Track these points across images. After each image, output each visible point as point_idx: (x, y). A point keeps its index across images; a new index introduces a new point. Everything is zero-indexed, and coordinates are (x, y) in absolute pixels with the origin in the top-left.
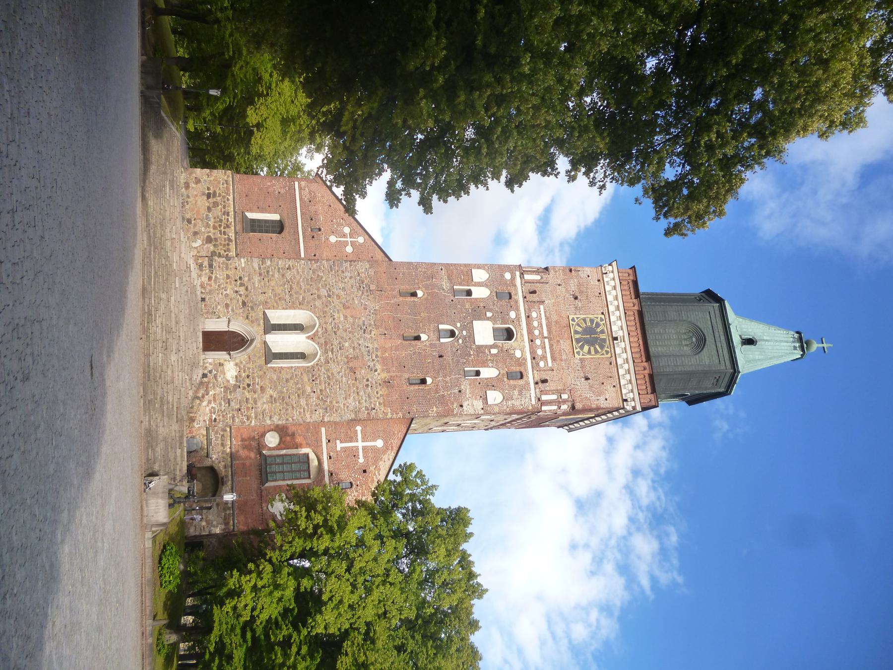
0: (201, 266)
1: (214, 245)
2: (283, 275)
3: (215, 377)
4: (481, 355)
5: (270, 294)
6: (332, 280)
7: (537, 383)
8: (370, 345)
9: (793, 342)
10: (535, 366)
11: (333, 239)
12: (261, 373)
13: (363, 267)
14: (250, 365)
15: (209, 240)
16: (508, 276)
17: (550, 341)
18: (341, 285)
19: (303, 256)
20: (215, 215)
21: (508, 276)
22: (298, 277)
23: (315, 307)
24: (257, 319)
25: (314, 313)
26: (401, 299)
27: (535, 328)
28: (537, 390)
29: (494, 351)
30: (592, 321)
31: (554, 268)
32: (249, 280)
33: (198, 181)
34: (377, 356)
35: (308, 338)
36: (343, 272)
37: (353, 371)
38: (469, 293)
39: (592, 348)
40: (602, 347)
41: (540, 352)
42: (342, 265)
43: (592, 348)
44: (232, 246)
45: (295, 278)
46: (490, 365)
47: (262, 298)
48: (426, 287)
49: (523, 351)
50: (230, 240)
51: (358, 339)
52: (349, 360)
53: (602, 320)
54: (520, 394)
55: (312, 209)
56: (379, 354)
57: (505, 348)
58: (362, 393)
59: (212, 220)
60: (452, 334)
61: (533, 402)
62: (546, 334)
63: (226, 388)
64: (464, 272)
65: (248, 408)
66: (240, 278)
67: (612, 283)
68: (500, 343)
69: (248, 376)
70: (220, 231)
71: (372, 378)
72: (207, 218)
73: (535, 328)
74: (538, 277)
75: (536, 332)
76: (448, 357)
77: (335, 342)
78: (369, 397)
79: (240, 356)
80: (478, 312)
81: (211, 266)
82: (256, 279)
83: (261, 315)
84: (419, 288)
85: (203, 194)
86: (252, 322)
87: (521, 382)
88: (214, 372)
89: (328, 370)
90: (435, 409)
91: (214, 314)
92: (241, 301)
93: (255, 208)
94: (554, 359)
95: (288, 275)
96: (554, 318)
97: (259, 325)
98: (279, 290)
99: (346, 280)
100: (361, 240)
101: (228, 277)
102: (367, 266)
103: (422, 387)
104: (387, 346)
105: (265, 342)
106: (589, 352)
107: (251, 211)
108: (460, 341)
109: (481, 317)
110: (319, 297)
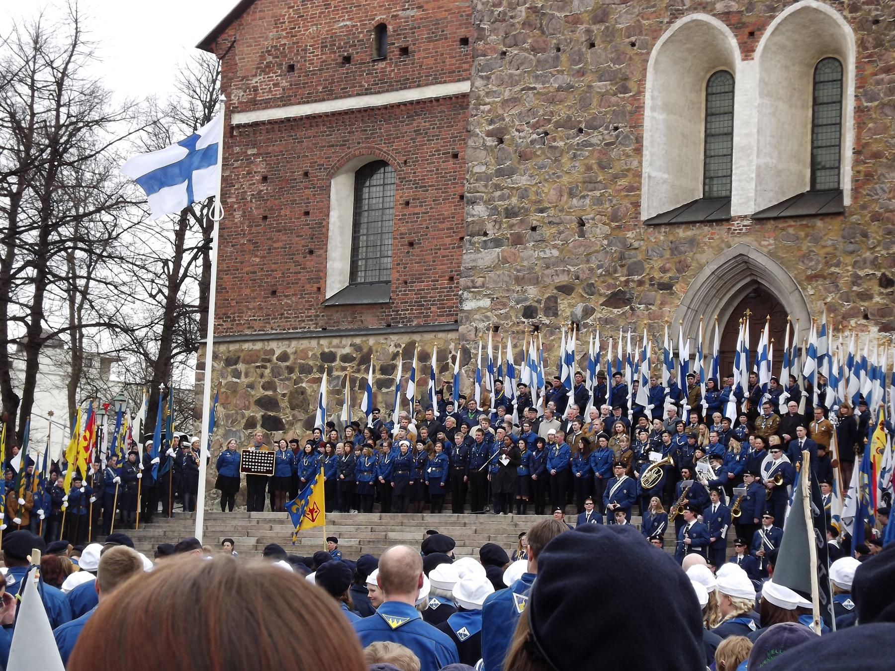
2: (523, 157)
14: (845, 274)
19: (463, 87)
22: (530, 100)
23: (637, 29)
24: (675, 250)
25: (656, 33)
32: (536, 281)
35: (747, 51)
47: (598, 231)
55: (315, 58)
66: (529, 312)
82: (530, 254)
83: (660, 236)
86: (682, 267)
93: (311, 263)
95: (522, 135)
97: (692, 242)
98: (573, 171)
105: (759, 219)
107: (319, 277)
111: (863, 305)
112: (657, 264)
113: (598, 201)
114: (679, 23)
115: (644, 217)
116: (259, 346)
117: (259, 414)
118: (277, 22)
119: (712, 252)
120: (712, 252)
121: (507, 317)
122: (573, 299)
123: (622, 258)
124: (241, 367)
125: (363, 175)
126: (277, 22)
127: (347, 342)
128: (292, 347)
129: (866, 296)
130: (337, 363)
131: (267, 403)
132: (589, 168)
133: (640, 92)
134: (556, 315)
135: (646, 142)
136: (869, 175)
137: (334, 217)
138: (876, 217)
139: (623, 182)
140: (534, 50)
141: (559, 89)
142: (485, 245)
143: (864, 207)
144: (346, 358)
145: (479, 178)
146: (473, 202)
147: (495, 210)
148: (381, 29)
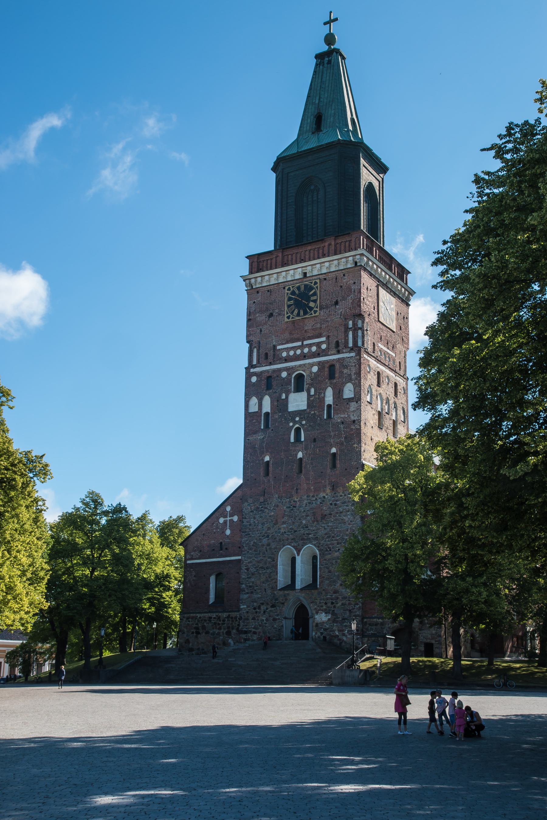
0: (246, 640)
1: (233, 629)
2: (253, 574)
3: (325, 630)
4: (315, 403)
7: (339, 352)
9: (323, 63)
10: (325, 353)
11: (228, 532)
12: (324, 593)
13: (247, 508)
15: (229, 633)
16: (254, 379)
17: (304, 339)
19: (240, 557)
21: (254, 379)
23: (275, 548)
24: (285, 596)
25: (280, 549)
26: (270, 475)
27: (295, 353)
28: (344, 351)
29: (312, 392)
30: (290, 299)
31: (248, 336)
32: (256, 602)
34: (313, 496)
35: (298, 554)
36: (250, 525)
37: (324, 517)
38: (267, 414)
39: (312, 298)
40: (311, 288)
41: (314, 349)
43: (312, 298)
44: (233, 614)
45: (254, 565)
46: (322, 395)
47: (269, 592)
48: (263, 454)
49: (312, 365)
50: (228, 617)
51: (300, 512)
52: (316, 520)
53: (289, 289)
54: (346, 367)
56: (311, 495)
57: (309, 381)
59: (215, 630)
60: (298, 431)
61: (353, 354)
62: (299, 343)
63: (334, 621)
64: (251, 419)
65: (350, 604)
66: (255, 609)
67: (259, 279)
68: (306, 386)
69: (326, 603)
70: (223, 624)
71: (330, 500)
72: (213, 634)
73: (295, 353)
74: (255, 350)
75: (299, 352)
78: (344, 503)
80: (280, 405)
81: (246, 632)
82: (255, 596)
84: (263, 460)
85: (196, 637)
86: (286, 599)
87: (337, 366)
88: (322, 630)
89: (323, 538)
90: (355, 445)
94: (320, 336)
95: (253, 570)
96: (287, 335)
97: (288, 594)
99: (256, 522)
100: (228, 509)
101: (254, 619)
102: (246, 504)
105: (302, 589)
106: (315, 301)
107: (208, 599)
108: (304, 422)
109: (285, 403)
110: (269, 545)
111: (322, 608)
112: (281, 599)
113: (269, 585)
116: (194, 615)
118: (197, 540)
123: (274, 597)
124: (190, 620)
125: (217, 576)
127: (215, 614)
128: (202, 615)
129: (322, 606)
130: (212, 619)
131: (197, 628)
132: (267, 577)
133: (277, 562)
135: (278, 572)
136: (322, 581)
137: (211, 585)
138: (324, 590)
139: (274, 581)
140: (255, 551)
142: (245, 594)
144: (214, 618)
145: (244, 579)
146: (242, 584)
147: (247, 586)
148: (221, 543)
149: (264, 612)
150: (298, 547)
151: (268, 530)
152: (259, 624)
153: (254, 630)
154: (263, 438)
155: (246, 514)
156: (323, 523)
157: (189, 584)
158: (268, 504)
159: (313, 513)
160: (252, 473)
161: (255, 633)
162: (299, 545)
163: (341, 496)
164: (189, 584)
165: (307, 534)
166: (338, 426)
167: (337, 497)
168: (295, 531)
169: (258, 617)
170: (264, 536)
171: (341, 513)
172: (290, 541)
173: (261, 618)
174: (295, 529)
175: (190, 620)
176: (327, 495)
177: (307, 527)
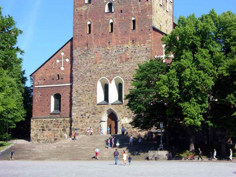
1: (67, 128)
5: (89, 101)
6: (83, 70)
8: (115, 51)
15: (64, 130)
18: (85, 65)
20: (52, 127)
22: (81, 87)
25: (99, 79)
32: (83, 111)
33: (36, 135)
35: (110, 82)
37: (127, 59)
42: (75, 64)
45: (81, 88)
47: (91, 105)
48: (86, 19)
50: (64, 120)
52: (122, 62)
56: (119, 45)
58: (138, 55)
66: (82, 115)
72: (54, 131)
76: (122, 7)
77: (113, 68)
79: (119, 116)
81: (76, 129)
82: (82, 108)
84: (86, 23)
85: (43, 132)
90: (148, 15)
91: (99, 129)
92: (92, 115)
93: (48, 107)
97: (104, 107)
98: (87, 97)
99: (82, 62)
101: (81, 121)
102: (76, 51)
103: (136, 23)
104: (115, 41)
107: (50, 109)
112: (99, 109)
114: (101, 78)
115: (98, 102)
117: (41, 129)
118: (42, 73)
119: (106, 108)
120: (106, 108)
121: (78, 116)
122: (88, 114)
124: (38, 122)
126: (42, 73)
128: (46, 119)
130: (53, 122)
134: (85, 116)
139: (94, 99)
140: (81, 80)
141: (85, 86)
143: (126, 103)
144: (54, 121)
148: (58, 75)
149: (88, 117)
150: (110, 78)
151: (90, 67)
152: (85, 125)
153: (81, 128)
154: (87, 9)
155: (75, 57)
156: (127, 64)
157: (37, 100)
158: (90, 51)
159: (120, 57)
160: (79, 31)
161: (82, 130)
162: (111, 77)
163: (138, 47)
164: (37, 100)
165: (116, 70)
166: (137, 3)
167: (136, 47)
168: (109, 68)
169: (85, 120)
170: (88, 71)
171: (138, 57)
172: (105, 74)
173: (86, 121)
174: (108, 67)
175: (38, 122)
176: (129, 46)
177: (116, 66)
